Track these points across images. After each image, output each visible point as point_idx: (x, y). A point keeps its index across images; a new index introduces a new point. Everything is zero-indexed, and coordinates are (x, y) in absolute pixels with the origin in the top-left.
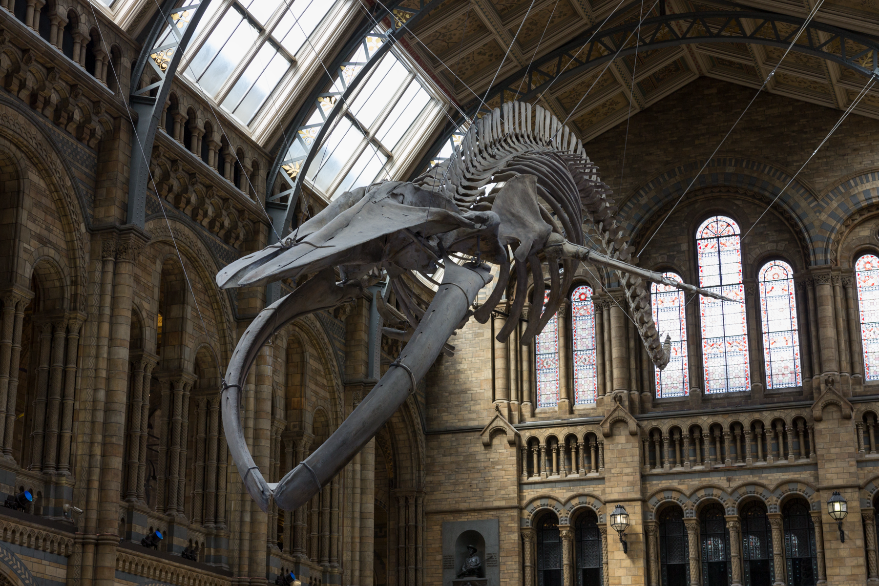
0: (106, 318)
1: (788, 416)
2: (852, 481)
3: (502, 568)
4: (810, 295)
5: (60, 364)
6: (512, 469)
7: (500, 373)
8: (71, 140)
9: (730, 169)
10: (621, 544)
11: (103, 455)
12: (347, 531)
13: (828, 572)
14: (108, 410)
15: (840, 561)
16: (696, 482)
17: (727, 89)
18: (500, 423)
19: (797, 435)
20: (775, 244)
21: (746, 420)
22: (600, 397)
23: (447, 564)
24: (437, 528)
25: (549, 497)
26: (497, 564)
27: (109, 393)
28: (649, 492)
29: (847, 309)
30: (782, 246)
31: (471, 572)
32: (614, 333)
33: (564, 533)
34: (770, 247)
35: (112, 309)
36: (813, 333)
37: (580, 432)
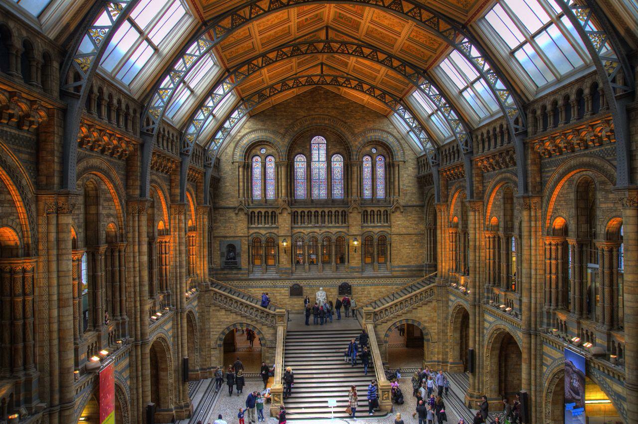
0: (137, 243)
1: (340, 210)
2: (360, 233)
3: (242, 257)
5: (117, 269)
6: (246, 223)
7: (241, 188)
8: (117, 161)
9: (327, 122)
11: (140, 305)
12: (198, 263)
13: (350, 262)
14: (141, 285)
16: (309, 230)
17: (327, 92)
19: (342, 216)
21: (326, 210)
23: (222, 255)
24: (218, 242)
27: (140, 277)
28: (293, 233)
29: (360, 174)
30: (341, 150)
31: (231, 259)
32: (283, 176)
34: (337, 150)
35: (139, 238)
37: (270, 211)
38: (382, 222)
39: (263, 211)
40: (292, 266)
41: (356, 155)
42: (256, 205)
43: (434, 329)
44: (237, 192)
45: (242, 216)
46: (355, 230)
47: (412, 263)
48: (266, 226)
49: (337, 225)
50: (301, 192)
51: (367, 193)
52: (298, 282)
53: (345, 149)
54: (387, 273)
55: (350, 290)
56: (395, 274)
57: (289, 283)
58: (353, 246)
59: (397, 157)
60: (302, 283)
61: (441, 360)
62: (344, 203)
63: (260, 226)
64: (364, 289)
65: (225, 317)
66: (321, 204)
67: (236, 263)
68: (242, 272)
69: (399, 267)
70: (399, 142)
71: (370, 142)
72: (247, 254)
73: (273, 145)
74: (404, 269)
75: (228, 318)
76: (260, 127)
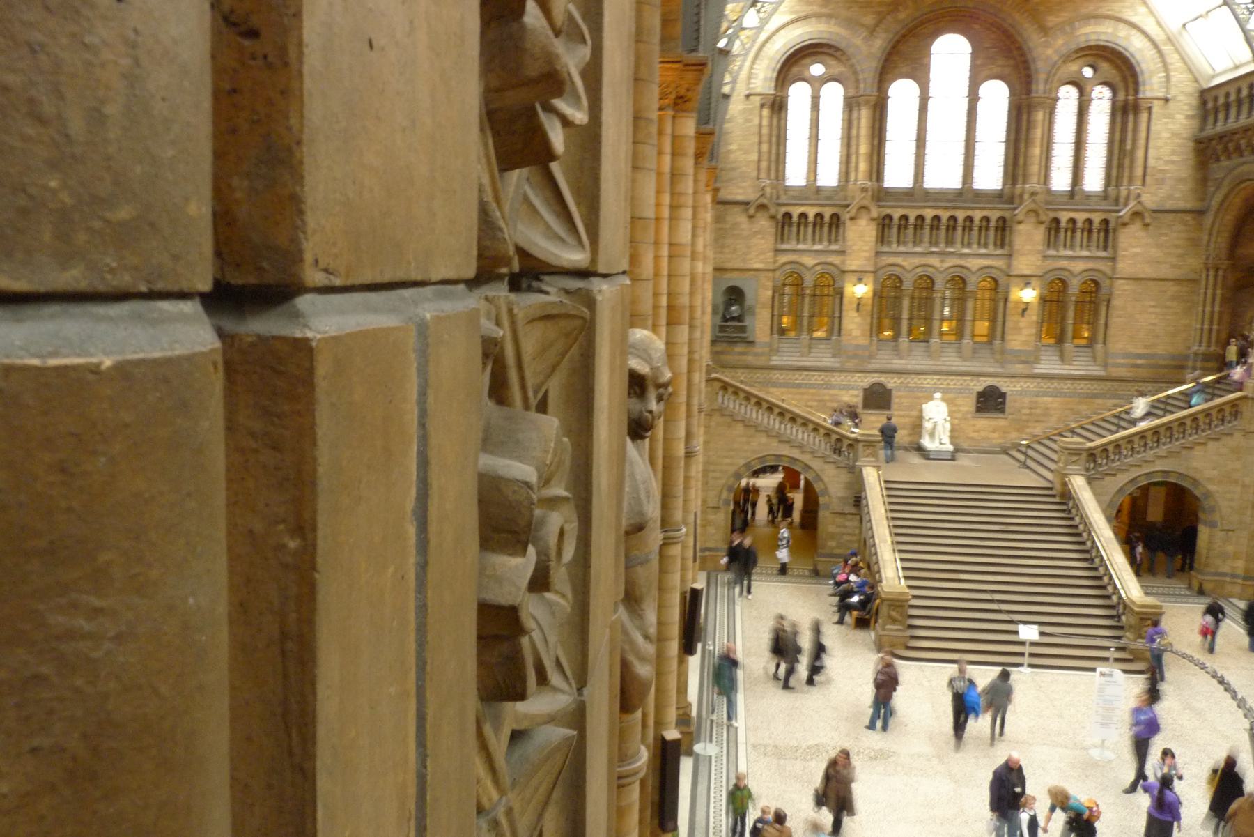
1: (994, 215)
4: (1025, 117)
6: (771, 239)
7: (765, 157)
10: (855, 306)
13: (1008, 337)
15: (1018, 330)
16: (917, 261)
18: (765, 201)
20: (999, 68)
21: (961, 215)
22: (842, 183)
25: (797, 263)
26: (753, 314)
30: (1007, 70)
31: (733, 319)
33: (808, 292)
36: (1022, 150)
37: (827, 213)
38: (1094, 248)
39: (811, 212)
40: (871, 341)
41: (1046, 82)
42: (794, 197)
43: (1232, 500)
44: (754, 166)
45: (763, 223)
46: (1024, 264)
47: (1160, 350)
48: (818, 247)
49: (983, 251)
50: (898, 175)
51: (1060, 181)
52: (882, 379)
53: (1016, 67)
54: (1096, 371)
55: (1003, 403)
56: (1116, 372)
57: (866, 381)
58: (1019, 302)
59: (1147, 87)
60: (891, 382)
61: (1240, 572)
62: (1005, 198)
63: (801, 246)
64: (1036, 402)
65: (744, 439)
66: (948, 201)
67: (743, 329)
68: (757, 349)
69: (1127, 355)
70: (1160, 52)
71: (1082, 49)
72: (770, 310)
73: (844, 53)
74: (1139, 362)
75: (748, 443)
76: (815, 9)
